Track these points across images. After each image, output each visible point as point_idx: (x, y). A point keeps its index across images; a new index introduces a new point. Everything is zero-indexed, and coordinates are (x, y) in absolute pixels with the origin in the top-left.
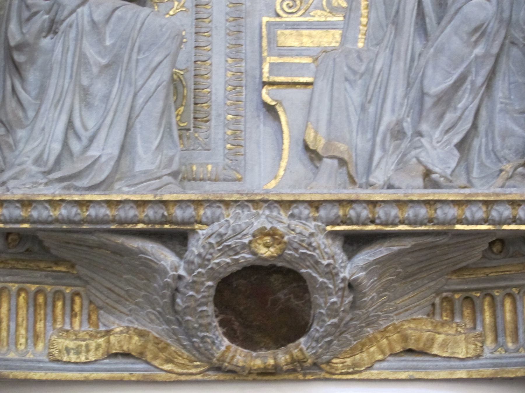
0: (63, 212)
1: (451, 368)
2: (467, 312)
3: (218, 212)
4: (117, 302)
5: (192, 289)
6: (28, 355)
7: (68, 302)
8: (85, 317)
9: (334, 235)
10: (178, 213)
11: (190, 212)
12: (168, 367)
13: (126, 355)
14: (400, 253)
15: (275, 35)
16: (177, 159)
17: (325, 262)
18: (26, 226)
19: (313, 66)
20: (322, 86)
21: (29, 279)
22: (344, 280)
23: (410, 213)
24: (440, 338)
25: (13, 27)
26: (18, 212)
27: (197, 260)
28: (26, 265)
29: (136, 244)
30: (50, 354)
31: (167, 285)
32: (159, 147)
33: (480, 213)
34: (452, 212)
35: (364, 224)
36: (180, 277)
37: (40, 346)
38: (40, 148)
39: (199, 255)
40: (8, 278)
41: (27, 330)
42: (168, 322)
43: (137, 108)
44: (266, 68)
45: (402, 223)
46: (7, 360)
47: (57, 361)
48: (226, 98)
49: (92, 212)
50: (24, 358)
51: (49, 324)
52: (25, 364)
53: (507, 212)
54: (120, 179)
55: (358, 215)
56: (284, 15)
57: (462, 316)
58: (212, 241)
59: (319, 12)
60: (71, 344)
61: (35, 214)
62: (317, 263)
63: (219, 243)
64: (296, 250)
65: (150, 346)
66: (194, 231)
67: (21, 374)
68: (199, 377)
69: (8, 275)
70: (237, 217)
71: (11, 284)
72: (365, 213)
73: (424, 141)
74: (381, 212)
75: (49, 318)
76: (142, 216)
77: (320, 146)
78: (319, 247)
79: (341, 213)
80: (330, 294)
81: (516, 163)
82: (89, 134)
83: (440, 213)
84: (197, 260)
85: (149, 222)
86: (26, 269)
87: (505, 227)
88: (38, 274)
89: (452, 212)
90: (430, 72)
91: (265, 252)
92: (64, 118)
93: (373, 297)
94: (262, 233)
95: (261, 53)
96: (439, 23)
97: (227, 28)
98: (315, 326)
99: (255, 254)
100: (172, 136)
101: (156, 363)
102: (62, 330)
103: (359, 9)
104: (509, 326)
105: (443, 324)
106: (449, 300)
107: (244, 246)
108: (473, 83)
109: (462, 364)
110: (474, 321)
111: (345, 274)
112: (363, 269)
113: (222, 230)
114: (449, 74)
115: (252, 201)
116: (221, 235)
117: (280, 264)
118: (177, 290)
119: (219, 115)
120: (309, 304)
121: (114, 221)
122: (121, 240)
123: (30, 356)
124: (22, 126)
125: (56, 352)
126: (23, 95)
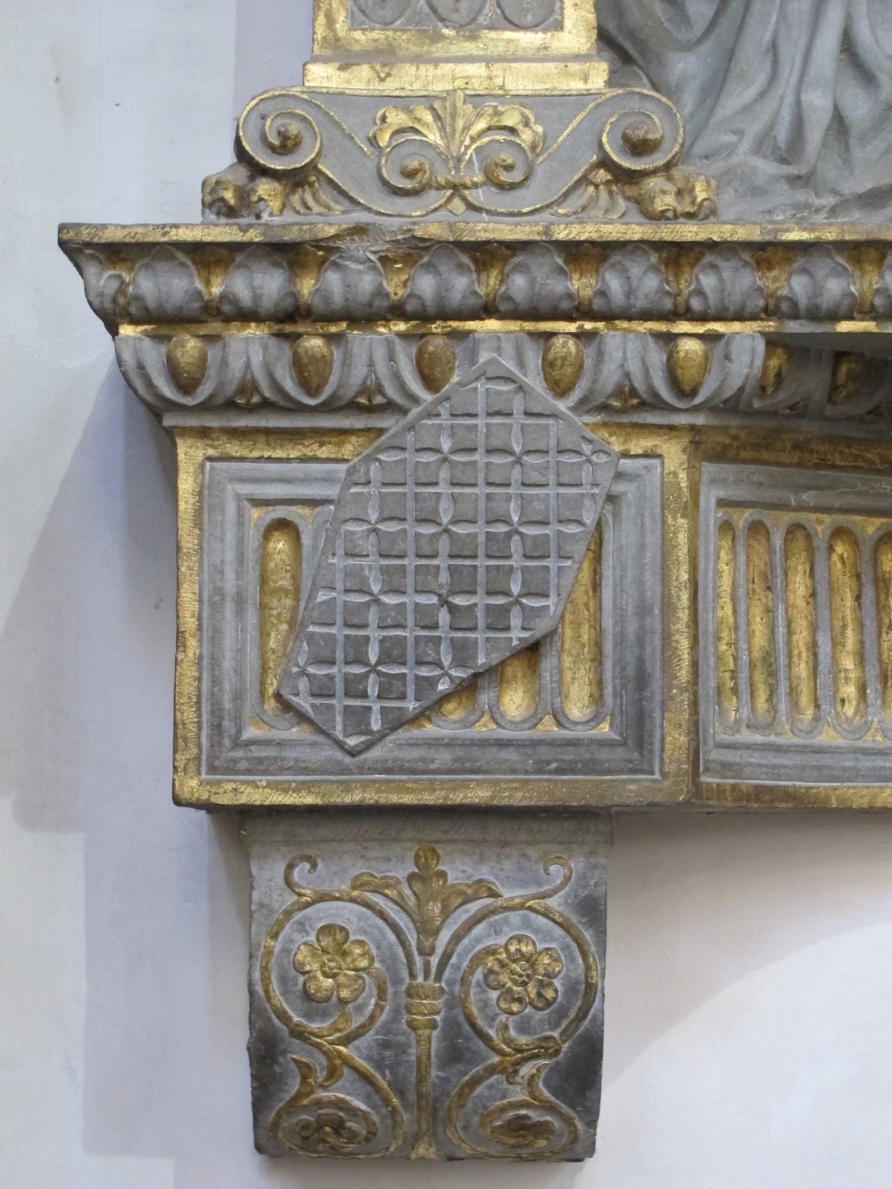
6: (869, 734)
21: (861, 502)
28: (856, 457)
40: (808, 497)
41: (861, 658)
46: (819, 750)
50: (859, 744)
52: (866, 763)
69: (807, 488)
71: (813, 516)
86: (856, 468)
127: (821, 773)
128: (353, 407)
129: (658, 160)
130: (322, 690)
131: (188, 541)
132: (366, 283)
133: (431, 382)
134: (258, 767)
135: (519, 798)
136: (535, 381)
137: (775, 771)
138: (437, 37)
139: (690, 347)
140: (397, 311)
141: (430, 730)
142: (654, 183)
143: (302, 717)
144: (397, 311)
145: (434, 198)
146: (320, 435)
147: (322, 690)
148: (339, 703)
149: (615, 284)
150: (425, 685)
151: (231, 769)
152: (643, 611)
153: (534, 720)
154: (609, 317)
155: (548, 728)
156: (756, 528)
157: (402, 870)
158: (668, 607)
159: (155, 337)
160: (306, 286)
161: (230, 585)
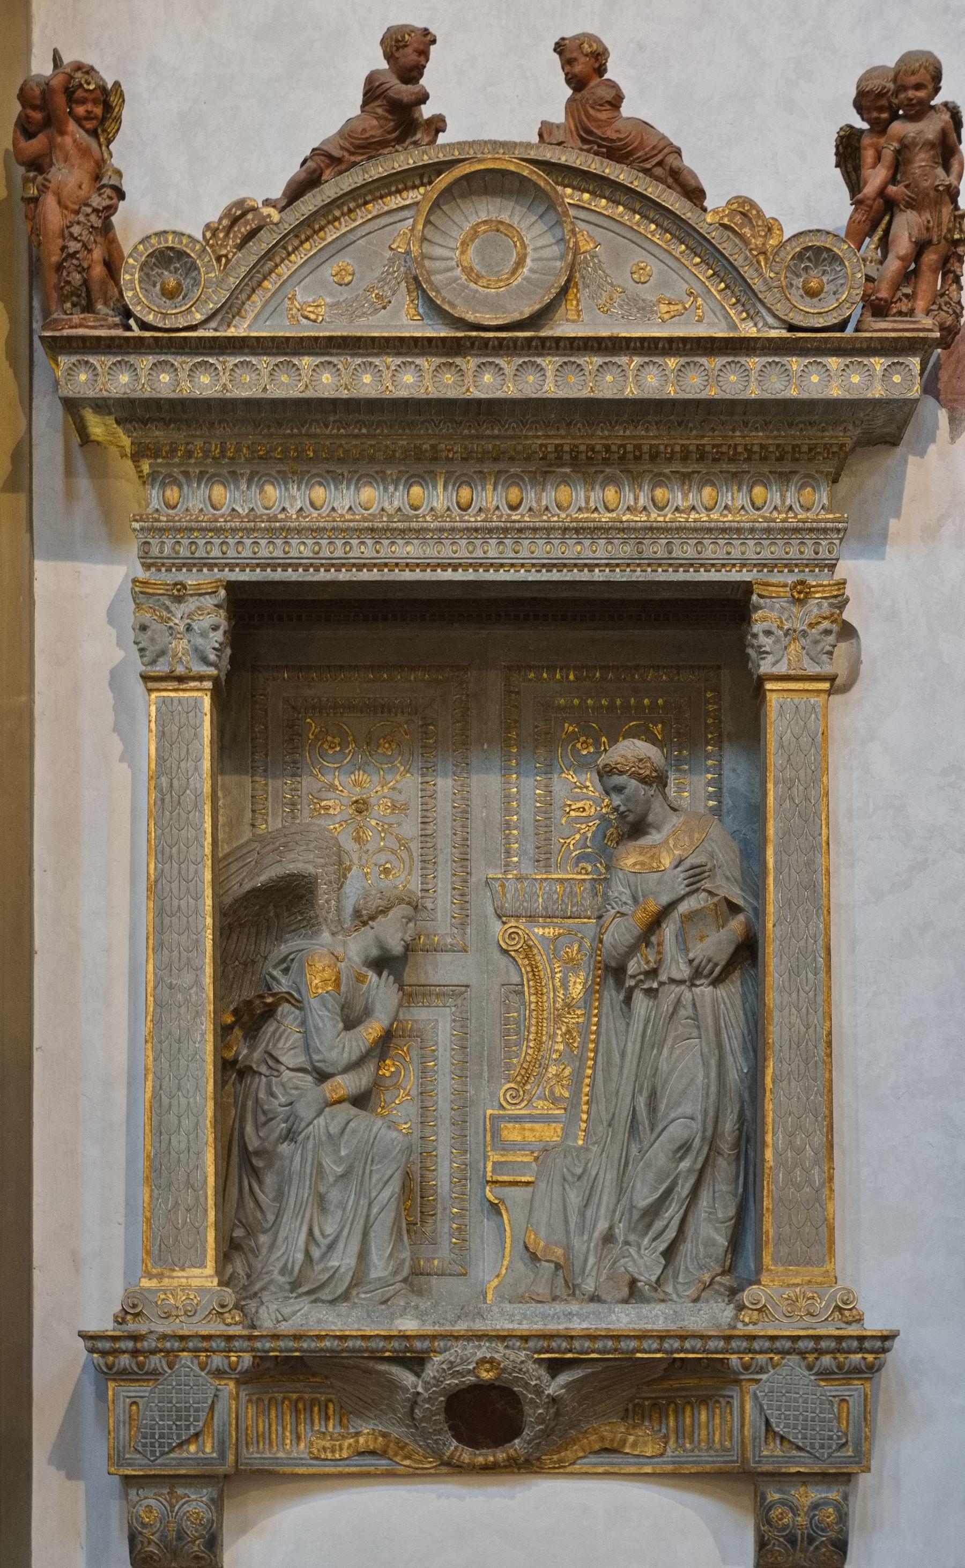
0: (327, 1344)
1: (639, 1464)
2: (655, 1416)
3: (449, 1344)
4: (365, 1408)
5: (428, 1402)
7: (323, 1408)
8: (338, 1420)
9: (539, 1361)
10: (418, 1345)
11: (427, 1344)
12: (407, 1462)
13: (372, 1453)
14: (593, 1374)
15: (500, 1129)
16: (407, 1264)
17: (533, 1383)
18: (297, 1354)
19: (534, 1165)
20: (542, 1185)
22: (549, 1395)
23: (599, 1345)
24: (631, 1438)
25: (249, 1129)
26: (291, 1344)
27: (432, 1381)
29: (383, 1367)
30: (311, 1452)
31: (408, 1400)
32: (391, 1255)
33: (655, 1346)
34: (633, 1344)
35: (564, 1353)
36: (418, 1393)
37: (302, 1445)
38: (285, 1257)
39: (434, 1378)
42: (408, 1426)
43: (372, 1218)
44: (489, 1168)
45: (593, 1352)
47: (317, 1458)
48: (451, 1190)
49: (350, 1344)
51: (308, 1427)
53: (677, 1344)
54: (356, 1285)
55: (559, 1347)
56: (508, 1107)
57: (651, 1419)
58: (444, 1366)
59: (541, 1102)
60: (328, 1444)
61: (305, 1345)
62: (527, 1383)
63: (449, 1369)
64: (510, 1374)
65: (392, 1445)
66: (430, 1358)
67: (288, 1470)
68: (432, 1471)
70: (464, 1348)
72: (564, 1345)
73: (632, 1251)
74: (577, 1344)
75: (308, 1422)
76: (389, 1347)
77: (539, 1245)
78: (528, 1371)
79: (545, 1344)
80: (538, 1407)
81: (714, 1273)
82: (328, 1241)
83: (623, 1345)
84: (432, 1381)
85: (395, 1351)
87: (676, 1356)
88: (298, 1385)
89: (633, 1344)
90: (639, 1185)
91: (485, 1375)
92: (305, 1229)
93: (574, 1408)
94: (483, 1361)
95: (485, 1146)
96: (652, 1130)
97: (452, 1118)
98: (526, 1431)
99: (478, 1377)
100: (402, 1240)
101: (398, 1459)
102: (319, 1432)
103: (579, 1104)
104: (688, 1429)
105: (634, 1427)
106: (641, 1406)
107: (469, 1371)
108: (679, 1194)
109: (648, 1460)
110: (660, 1424)
111: (550, 1391)
112: (563, 1387)
113: (452, 1359)
114: (656, 1189)
115: (476, 1336)
116: (451, 1363)
117: (497, 1383)
118: (416, 1403)
119: (445, 1209)
120: (521, 1412)
121: (366, 1350)
122: (371, 1364)
123: (295, 1455)
124: (265, 1232)
125: (316, 1452)
126: (261, 1197)
127: (277, 1464)
128: (151, 1374)
129: (227, 1309)
130: (144, 1445)
131: (111, 1407)
132: (154, 1344)
133: (170, 1368)
134: (129, 1465)
135: (193, 1472)
136: (196, 1368)
137: (263, 1464)
138: (174, 1270)
139: (234, 1359)
140: (161, 1351)
141: (172, 1455)
142: (226, 1315)
143: (139, 1452)
144: (161, 1351)
145: (171, 1319)
146: (144, 1380)
147: (144, 1445)
148: (149, 1449)
149: (214, 1345)
150: (170, 1444)
151: (122, 1465)
152: (224, 1425)
153: (197, 1453)
154: (214, 1352)
155: (201, 1455)
156: (259, 1399)
157: (166, 1491)
158: (230, 1424)
159: (103, 1357)
160: (139, 1345)
161: (122, 1419)
